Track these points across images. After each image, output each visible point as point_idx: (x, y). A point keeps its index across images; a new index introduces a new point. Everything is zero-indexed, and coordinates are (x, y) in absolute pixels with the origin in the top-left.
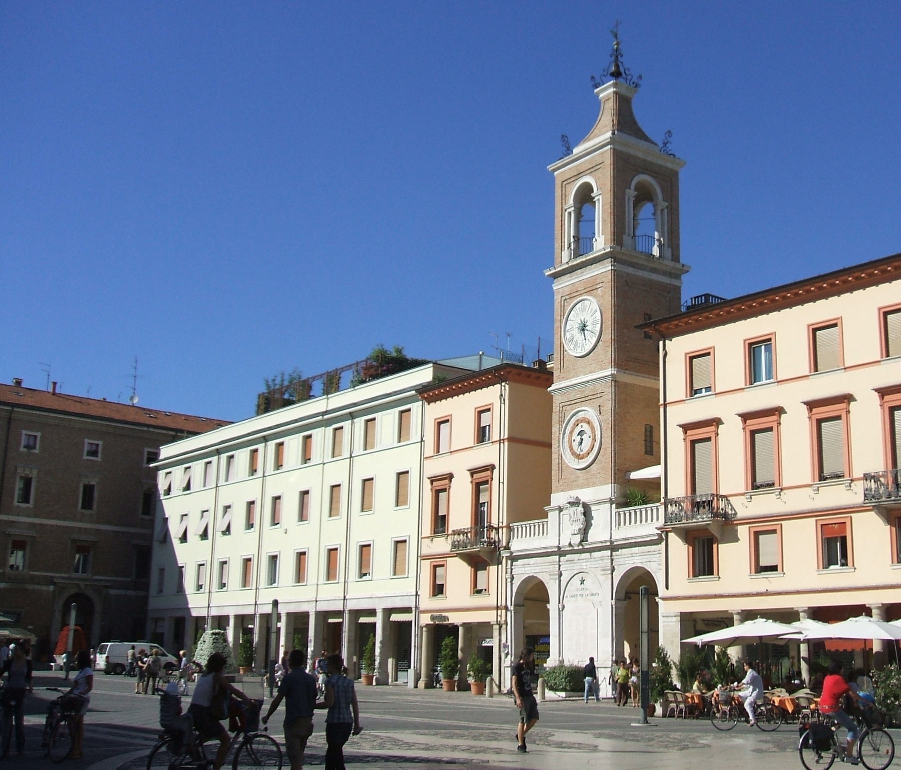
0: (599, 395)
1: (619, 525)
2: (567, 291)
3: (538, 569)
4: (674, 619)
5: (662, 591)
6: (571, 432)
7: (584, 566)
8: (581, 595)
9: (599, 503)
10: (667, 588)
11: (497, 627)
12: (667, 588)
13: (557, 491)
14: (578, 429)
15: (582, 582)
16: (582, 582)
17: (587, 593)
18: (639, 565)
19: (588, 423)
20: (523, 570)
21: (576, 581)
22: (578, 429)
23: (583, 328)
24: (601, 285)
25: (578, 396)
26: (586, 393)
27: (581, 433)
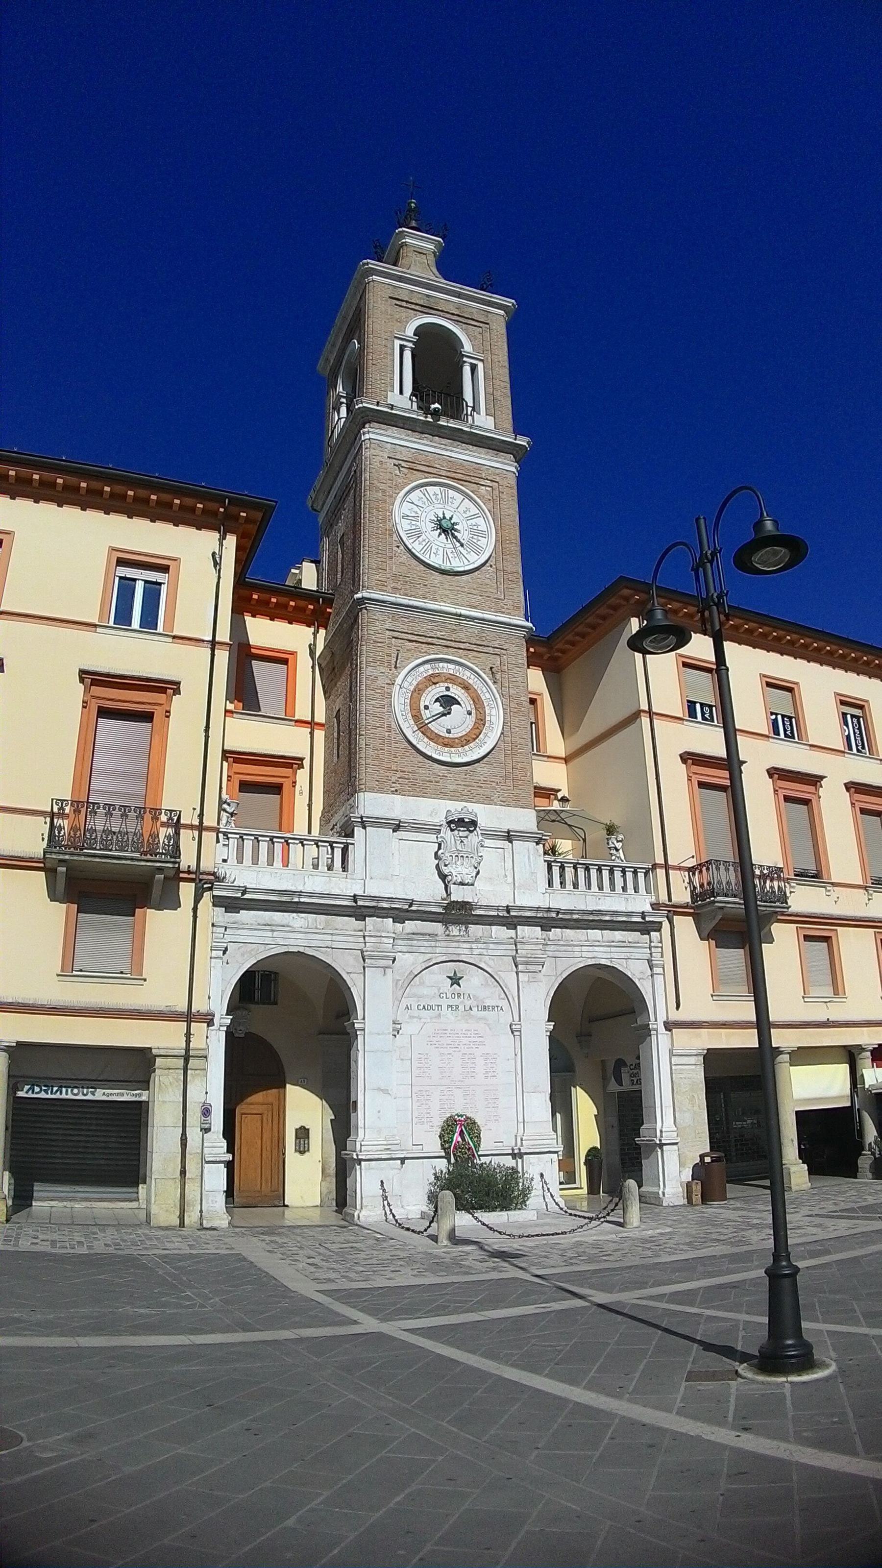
0: (491, 650)
1: (550, 883)
2: (405, 455)
3: (319, 940)
4: (693, 1060)
5: (660, 1008)
6: (418, 691)
7: (463, 951)
8: (454, 1008)
9: (509, 837)
10: (678, 1006)
11: (181, 1062)
12: (678, 1006)
13: (381, 791)
14: (439, 690)
15: (455, 980)
16: (455, 980)
17: (468, 1003)
18: (603, 962)
19: (466, 687)
20: (260, 938)
21: (439, 977)
22: (439, 690)
23: (446, 529)
24: (489, 483)
25: (439, 634)
26: (462, 636)
27: (448, 702)
